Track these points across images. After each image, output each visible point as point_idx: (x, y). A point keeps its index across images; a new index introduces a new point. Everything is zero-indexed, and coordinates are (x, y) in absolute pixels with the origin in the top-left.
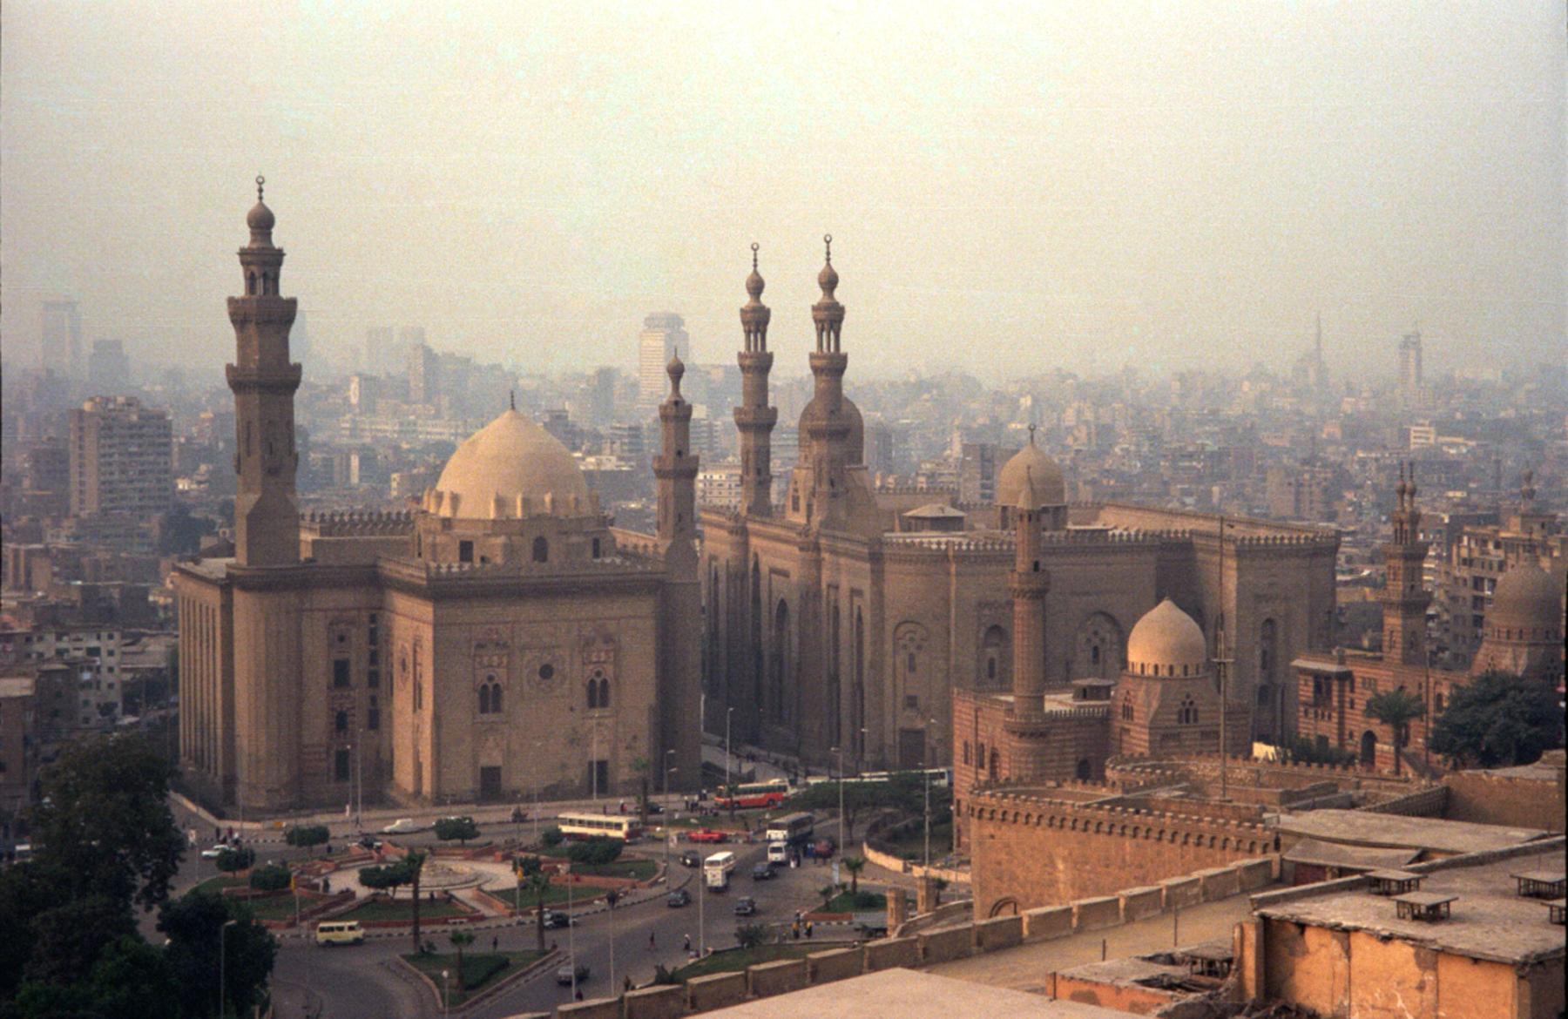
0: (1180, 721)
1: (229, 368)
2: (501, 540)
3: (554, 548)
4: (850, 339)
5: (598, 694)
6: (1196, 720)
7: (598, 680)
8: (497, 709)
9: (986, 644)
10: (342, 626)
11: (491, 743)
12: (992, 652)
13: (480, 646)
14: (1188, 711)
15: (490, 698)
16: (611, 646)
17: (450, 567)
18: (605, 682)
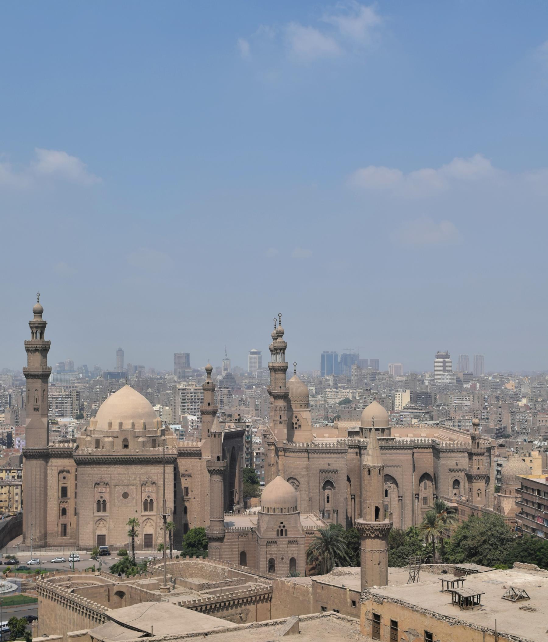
0: (278, 535)
1: (24, 368)
2: (111, 439)
3: (131, 445)
4: (289, 357)
5: (148, 505)
6: (286, 535)
7: (149, 500)
8: (104, 510)
9: (324, 489)
10: (65, 473)
11: (101, 525)
12: (327, 492)
13: (96, 483)
14: (282, 530)
15: (102, 505)
16: (154, 485)
18: (151, 500)
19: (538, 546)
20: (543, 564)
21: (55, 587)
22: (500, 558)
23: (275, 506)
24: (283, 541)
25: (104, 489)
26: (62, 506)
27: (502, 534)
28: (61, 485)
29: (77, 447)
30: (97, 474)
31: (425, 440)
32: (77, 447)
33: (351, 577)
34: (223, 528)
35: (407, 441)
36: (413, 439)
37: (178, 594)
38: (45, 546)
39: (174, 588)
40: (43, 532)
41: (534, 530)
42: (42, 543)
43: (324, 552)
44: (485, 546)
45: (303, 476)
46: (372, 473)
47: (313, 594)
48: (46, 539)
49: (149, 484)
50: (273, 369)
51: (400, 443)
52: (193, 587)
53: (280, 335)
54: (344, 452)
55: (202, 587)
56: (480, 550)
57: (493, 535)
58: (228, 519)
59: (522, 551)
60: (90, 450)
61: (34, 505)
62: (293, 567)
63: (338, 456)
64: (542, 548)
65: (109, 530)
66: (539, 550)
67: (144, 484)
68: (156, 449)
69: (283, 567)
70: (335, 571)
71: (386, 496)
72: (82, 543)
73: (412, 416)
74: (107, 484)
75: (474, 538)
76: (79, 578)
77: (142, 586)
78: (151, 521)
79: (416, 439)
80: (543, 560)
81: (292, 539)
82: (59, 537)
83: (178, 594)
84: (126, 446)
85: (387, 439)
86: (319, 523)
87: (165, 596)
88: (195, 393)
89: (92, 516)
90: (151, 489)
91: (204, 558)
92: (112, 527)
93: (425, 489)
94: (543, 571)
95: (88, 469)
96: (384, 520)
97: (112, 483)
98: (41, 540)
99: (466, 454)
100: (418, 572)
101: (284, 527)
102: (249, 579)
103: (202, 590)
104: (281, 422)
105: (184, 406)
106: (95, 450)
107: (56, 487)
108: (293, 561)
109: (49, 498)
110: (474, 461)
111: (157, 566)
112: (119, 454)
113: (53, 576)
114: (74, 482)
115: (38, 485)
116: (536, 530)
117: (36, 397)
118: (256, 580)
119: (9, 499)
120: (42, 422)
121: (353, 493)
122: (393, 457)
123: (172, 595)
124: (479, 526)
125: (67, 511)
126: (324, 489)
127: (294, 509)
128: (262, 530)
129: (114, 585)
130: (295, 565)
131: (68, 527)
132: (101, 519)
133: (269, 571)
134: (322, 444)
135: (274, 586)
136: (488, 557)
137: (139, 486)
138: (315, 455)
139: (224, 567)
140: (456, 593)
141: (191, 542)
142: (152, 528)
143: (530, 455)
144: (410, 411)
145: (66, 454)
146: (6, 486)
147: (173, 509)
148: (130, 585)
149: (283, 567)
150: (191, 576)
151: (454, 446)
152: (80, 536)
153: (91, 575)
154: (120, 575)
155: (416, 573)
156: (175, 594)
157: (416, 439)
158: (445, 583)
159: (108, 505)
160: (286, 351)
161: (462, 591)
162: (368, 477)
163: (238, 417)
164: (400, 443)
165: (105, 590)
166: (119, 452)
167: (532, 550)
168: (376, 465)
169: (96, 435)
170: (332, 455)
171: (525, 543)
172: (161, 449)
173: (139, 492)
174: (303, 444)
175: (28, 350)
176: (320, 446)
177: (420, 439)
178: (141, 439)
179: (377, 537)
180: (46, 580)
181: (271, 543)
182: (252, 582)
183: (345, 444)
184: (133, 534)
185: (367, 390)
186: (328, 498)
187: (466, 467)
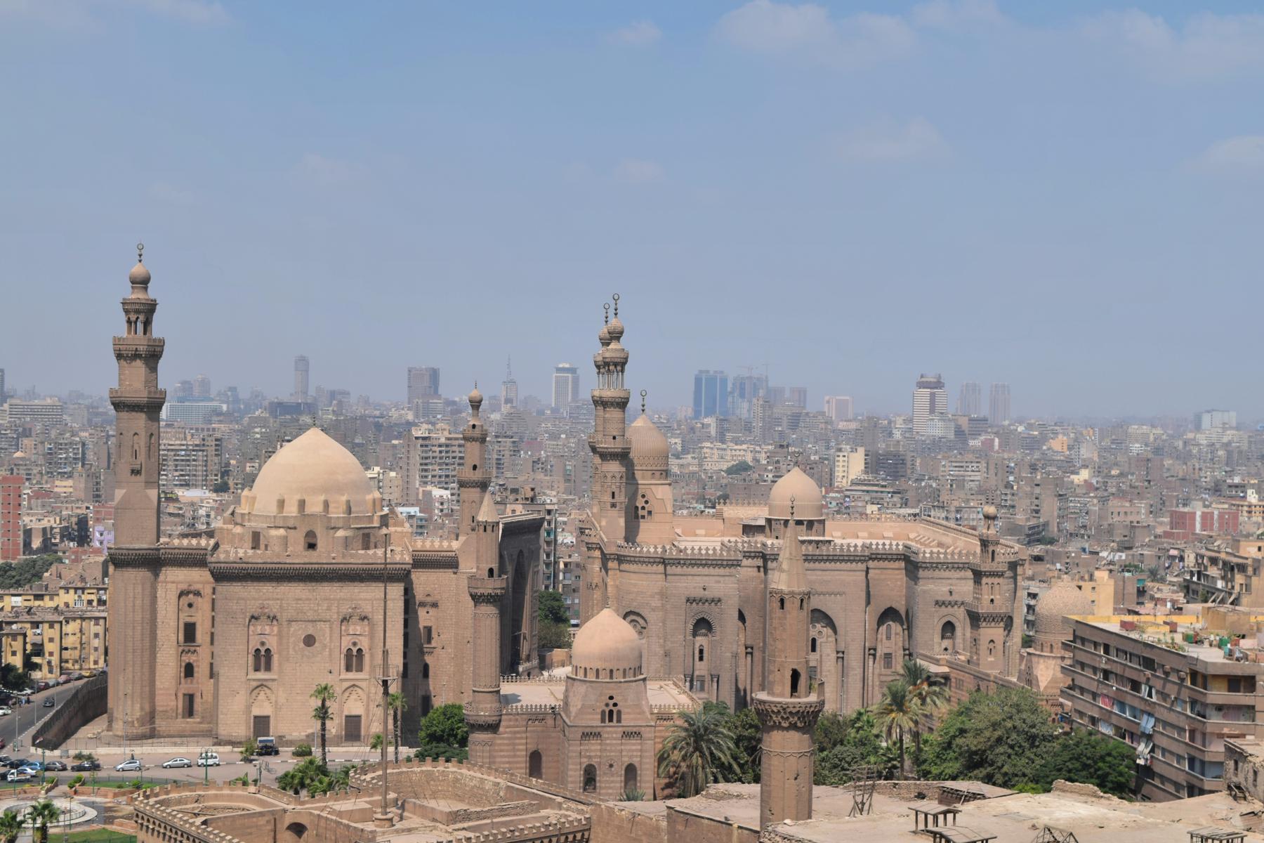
0: (603, 721)
2: (282, 532)
4: (632, 380)
5: (354, 660)
6: (619, 721)
8: (268, 668)
9: (695, 634)
10: (191, 596)
11: (262, 696)
12: (700, 640)
13: (253, 617)
14: (611, 712)
15: (263, 659)
16: (366, 622)
17: (245, 553)
18: (360, 650)
19: (1101, 750)
20: (1110, 785)
21: (169, 814)
22: (1027, 771)
23: (599, 665)
24: (612, 732)
25: (267, 628)
26: (187, 658)
27: (1033, 726)
28: (185, 618)
29: (217, 546)
30: (255, 599)
31: (891, 545)
32: (217, 546)
33: (743, 802)
34: (498, 705)
35: (856, 546)
36: (868, 541)
37: (409, 830)
38: (152, 735)
39: (401, 818)
40: (147, 708)
41: (1094, 721)
42: (145, 729)
43: (691, 756)
44: (1000, 749)
45: (653, 610)
46: (787, 605)
47: (669, 833)
48: (154, 723)
49: (355, 619)
50: (600, 403)
51: (842, 549)
52: (438, 817)
53: (616, 335)
54: (736, 564)
55: (454, 817)
56: (991, 757)
57: (1015, 727)
58: (507, 688)
59: (1071, 759)
60: (241, 553)
61: (130, 657)
62: (631, 782)
63: (722, 571)
64: (1109, 755)
65: (277, 707)
66: (1102, 758)
67: (345, 620)
68: (371, 552)
69: (611, 782)
70: (712, 791)
71: (814, 649)
72: (223, 731)
73: (867, 498)
74: (274, 618)
75: (978, 732)
76: (216, 797)
77: (340, 814)
78: (359, 691)
79: (874, 542)
80: (1110, 778)
81: (630, 730)
82: (180, 720)
83: (409, 830)
84: (312, 546)
85: (817, 542)
86: (684, 699)
87: (384, 833)
88: (447, 446)
89: (243, 679)
90: (358, 629)
91: (460, 762)
92: (282, 700)
93: (888, 638)
94: (1108, 799)
95: (236, 589)
96: (807, 696)
97: (283, 617)
98: (143, 725)
99: (970, 574)
100: (871, 795)
101: (615, 705)
102: (545, 803)
103: (455, 823)
104: (613, 505)
105: (426, 470)
106: (250, 552)
107: (173, 624)
108: (631, 771)
109: (159, 643)
110: (984, 587)
111: (368, 777)
112: (297, 561)
113: (167, 793)
114: (209, 614)
115: (138, 617)
116: (1099, 720)
117: (136, 447)
118: (560, 806)
119: (81, 644)
120: (147, 497)
121: (749, 643)
122: (828, 576)
123: (397, 831)
124: (991, 710)
125: (196, 669)
126: (695, 634)
127: (635, 671)
128: (573, 710)
129: (285, 811)
130: (635, 779)
131: (197, 700)
132: (262, 685)
133: (585, 790)
134: (693, 549)
135: (594, 817)
136: (1005, 769)
137: (336, 625)
138: (679, 570)
139: (498, 780)
140: (942, 836)
141: (433, 731)
142: (359, 703)
143: (1091, 578)
144: (865, 488)
145: (195, 560)
146: (74, 619)
147: (401, 669)
148: (316, 812)
149: (611, 782)
150: (434, 795)
151: (946, 557)
152: (221, 716)
153: (240, 792)
154: (297, 792)
155: (866, 796)
156: (403, 831)
157: (874, 542)
158: (921, 817)
159: (275, 659)
160: (626, 367)
161: (954, 833)
162: (779, 612)
163: (530, 494)
164: (842, 549)
165: (268, 822)
166: (298, 556)
167: (1088, 758)
168: (796, 589)
169: (253, 524)
170: (711, 571)
171: (1077, 745)
172: (380, 552)
173: (336, 635)
174: (656, 547)
175: (119, 356)
176: (689, 552)
177: (881, 542)
178: (340, 533)
179: (793, 727)
180: (152, 801)
181: (590, 735)
182: (553, 808)
183: (736, 550)
184: (323, 714)
185: (782, 446)
186: (701, 651)
187: (969, 599)
